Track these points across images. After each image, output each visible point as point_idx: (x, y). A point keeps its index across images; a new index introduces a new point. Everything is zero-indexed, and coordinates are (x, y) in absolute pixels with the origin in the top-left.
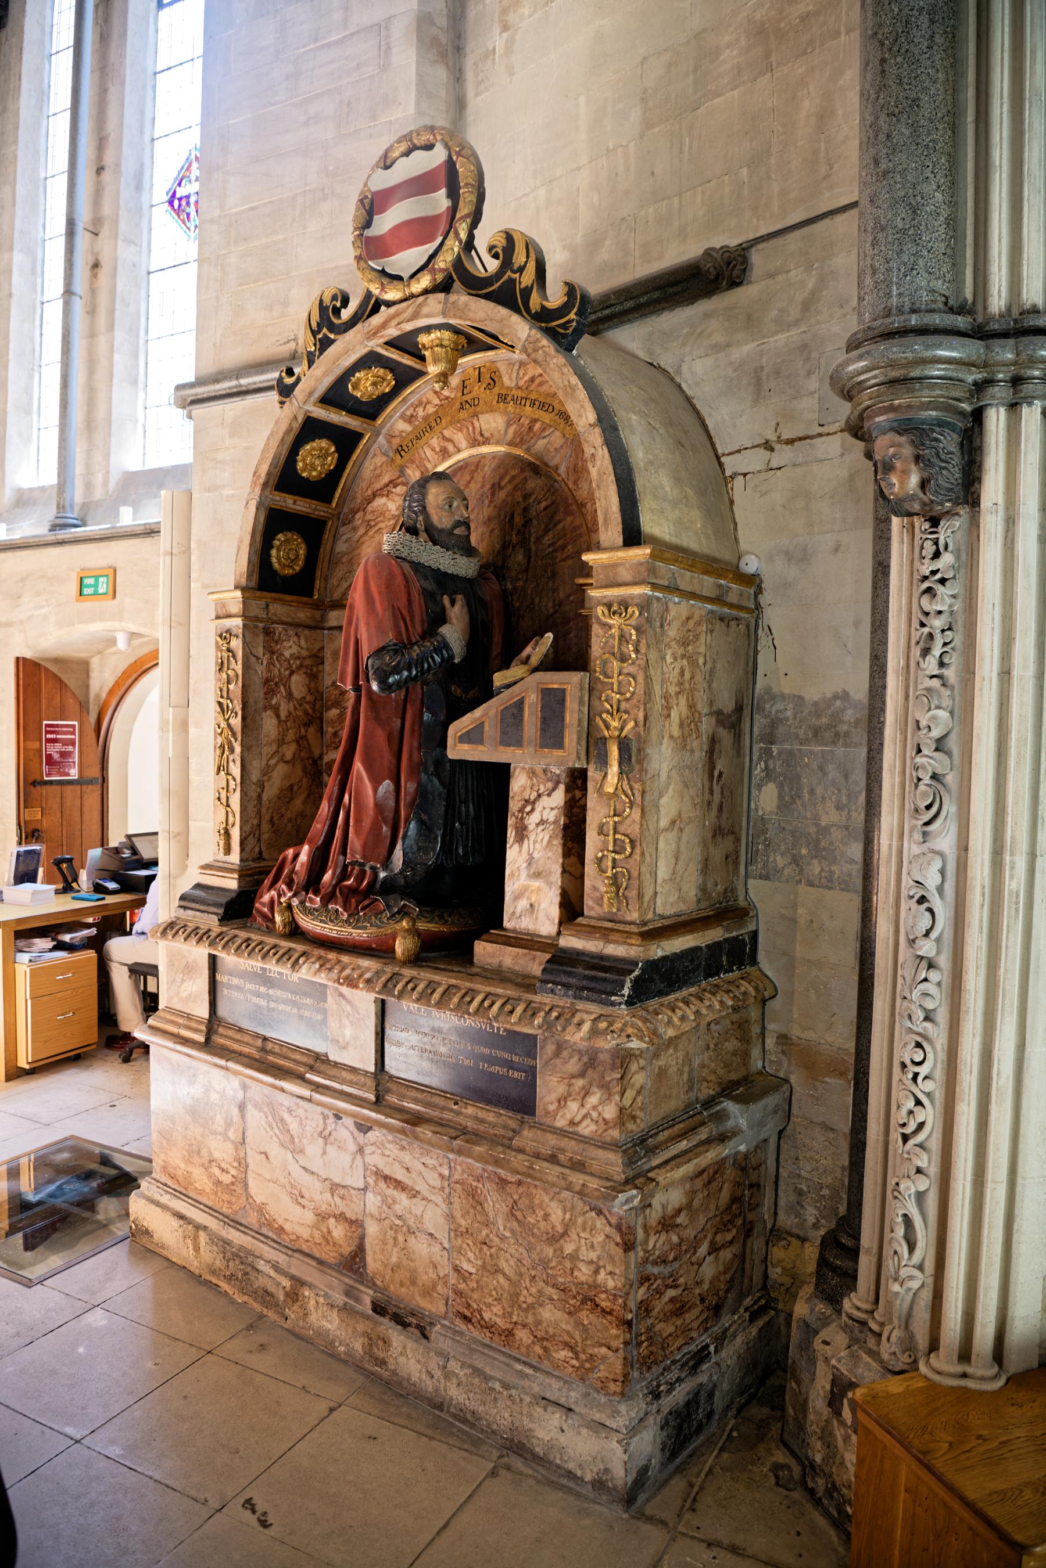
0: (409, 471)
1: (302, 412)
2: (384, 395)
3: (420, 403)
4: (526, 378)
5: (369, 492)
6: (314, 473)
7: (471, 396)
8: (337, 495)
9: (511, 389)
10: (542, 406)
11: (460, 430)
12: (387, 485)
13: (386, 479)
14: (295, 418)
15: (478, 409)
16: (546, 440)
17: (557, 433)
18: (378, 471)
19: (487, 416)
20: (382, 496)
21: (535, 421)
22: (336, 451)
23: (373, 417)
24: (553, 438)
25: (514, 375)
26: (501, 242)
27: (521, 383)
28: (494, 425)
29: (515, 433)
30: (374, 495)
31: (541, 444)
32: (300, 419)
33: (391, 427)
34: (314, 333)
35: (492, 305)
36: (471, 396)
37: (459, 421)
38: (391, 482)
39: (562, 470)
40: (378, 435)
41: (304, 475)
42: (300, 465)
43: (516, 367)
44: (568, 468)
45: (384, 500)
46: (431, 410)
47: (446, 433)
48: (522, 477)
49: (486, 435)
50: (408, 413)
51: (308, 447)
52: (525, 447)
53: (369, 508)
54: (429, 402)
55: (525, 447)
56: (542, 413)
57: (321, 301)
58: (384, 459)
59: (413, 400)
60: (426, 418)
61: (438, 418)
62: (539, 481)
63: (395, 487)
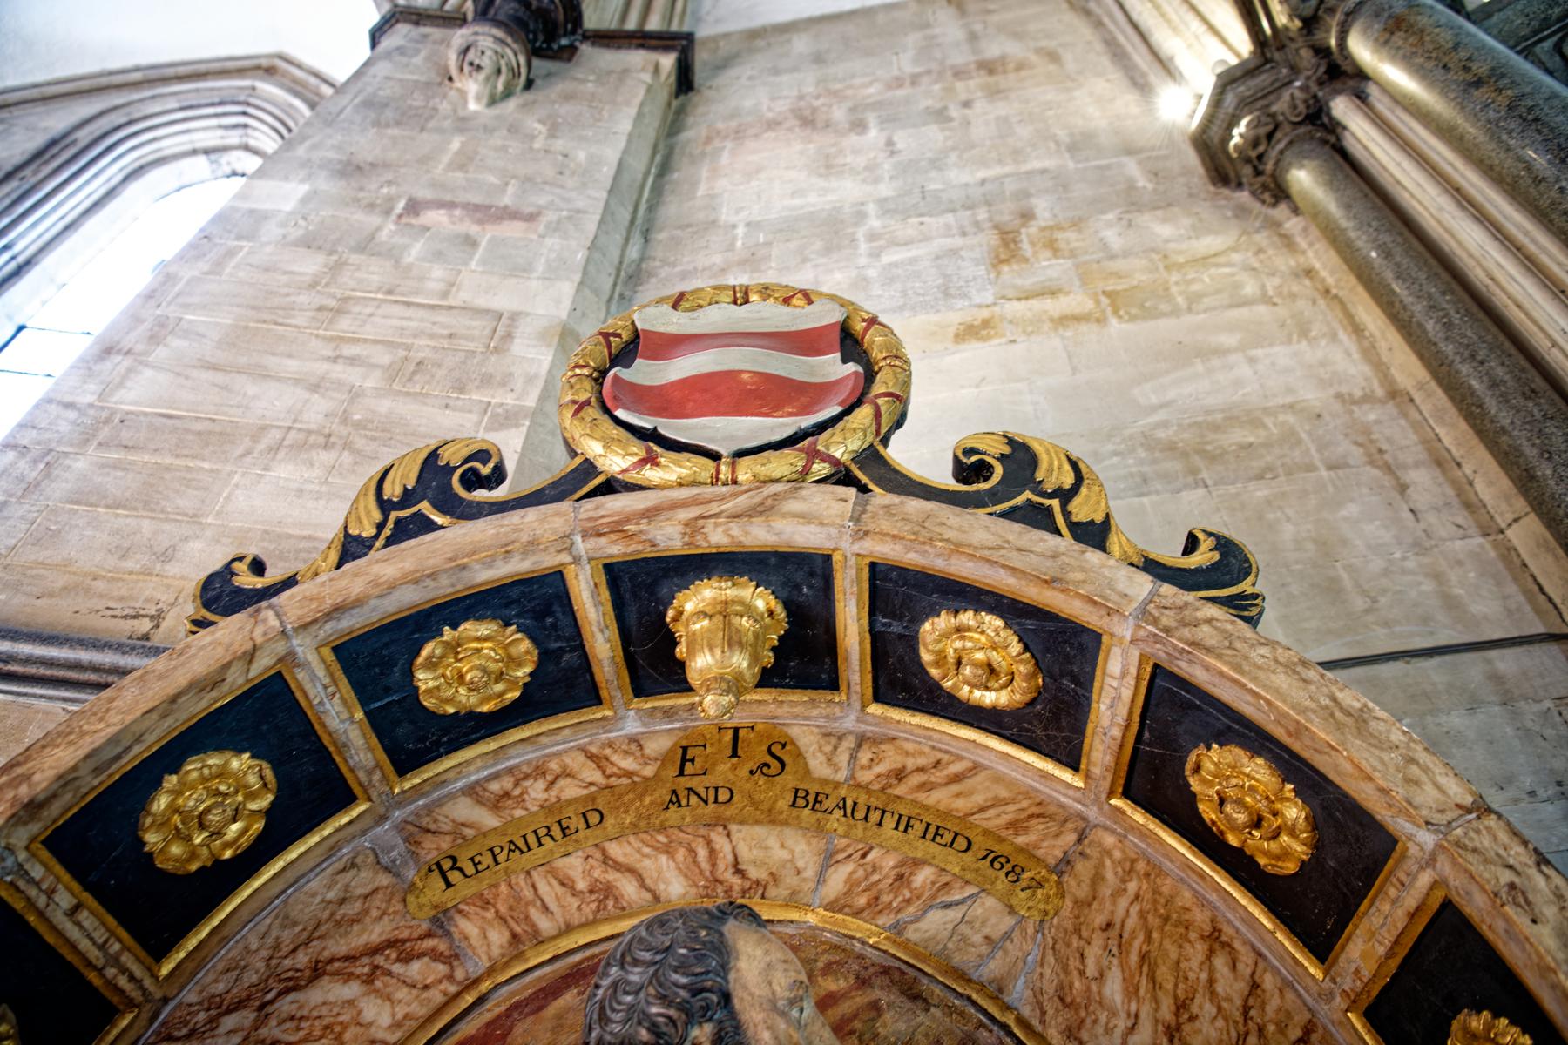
0: (467, 927)
1: (280, 648)
2: (471, 715)
3: (540, 771)
4: (881, 768)
5: (302, 959)
6: (176, 850)
7: (709, 780)
8: (192, 942)
9: (837, 785)
10: (933, 833)
11: (668, 850)
12: (376, 950)
13: (376, 933)
14: (250, 656)
15: (729, 811)
16: (954, 914)
17: (990, 902)
18: (352, 909)
19: (759, 831)
20: (348, 977)
21: (917, 863)
22: (269, 813)
23: (405, 762)
24: (977, 910)
25: (843, 758)
26: (994, 448)
27: (865, 777)
28: (780, 854)
29: (851, 884)
30: (317, 971)
31: (936, 923)
32: (262, 666)
33: (429, 809)
34: (385, 506)
35: (1017, 527)
36: (709, 780)
37: (662, 829)
38: (390, 944)
39: (1018, 993)
40: (383, 818)
41: (152, 839)
42: (161, 802)
43: (849, 743)
44: (1038, 994)
45: (352, 990)
46: (570, 790)
47: (614, 850)
48: (860, 999)
49: (754, 873)
50: (495, 787)
51: (214, 760)
52: (885, 920)
53: (286, 1005)
54: (566, 773)
55: (885, 920)
56: (934, 848)
57: (434, 455)
58: (384, 880)
59: (522, 757)
60: (547, 808)
61: (592, 812)
62: (921, 1017)
63: (406, 959)
